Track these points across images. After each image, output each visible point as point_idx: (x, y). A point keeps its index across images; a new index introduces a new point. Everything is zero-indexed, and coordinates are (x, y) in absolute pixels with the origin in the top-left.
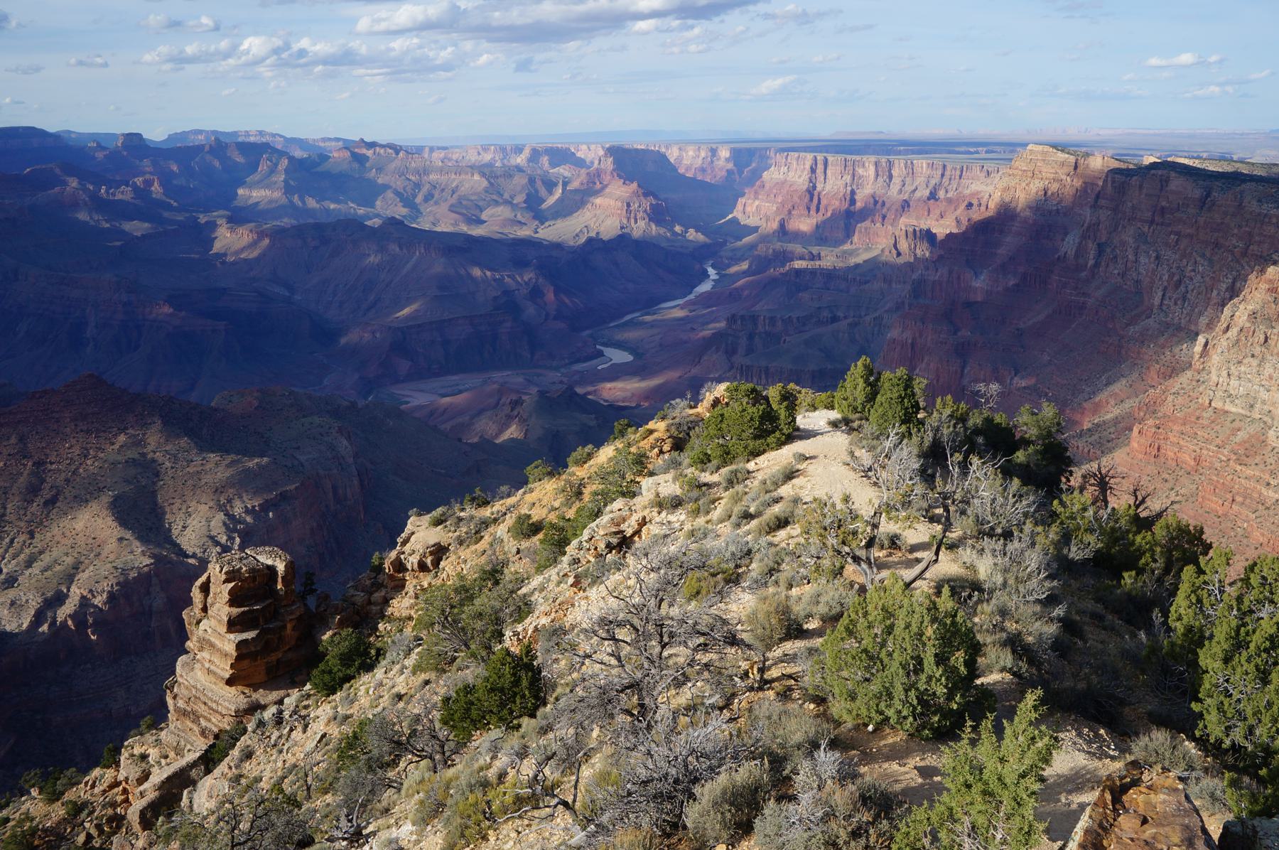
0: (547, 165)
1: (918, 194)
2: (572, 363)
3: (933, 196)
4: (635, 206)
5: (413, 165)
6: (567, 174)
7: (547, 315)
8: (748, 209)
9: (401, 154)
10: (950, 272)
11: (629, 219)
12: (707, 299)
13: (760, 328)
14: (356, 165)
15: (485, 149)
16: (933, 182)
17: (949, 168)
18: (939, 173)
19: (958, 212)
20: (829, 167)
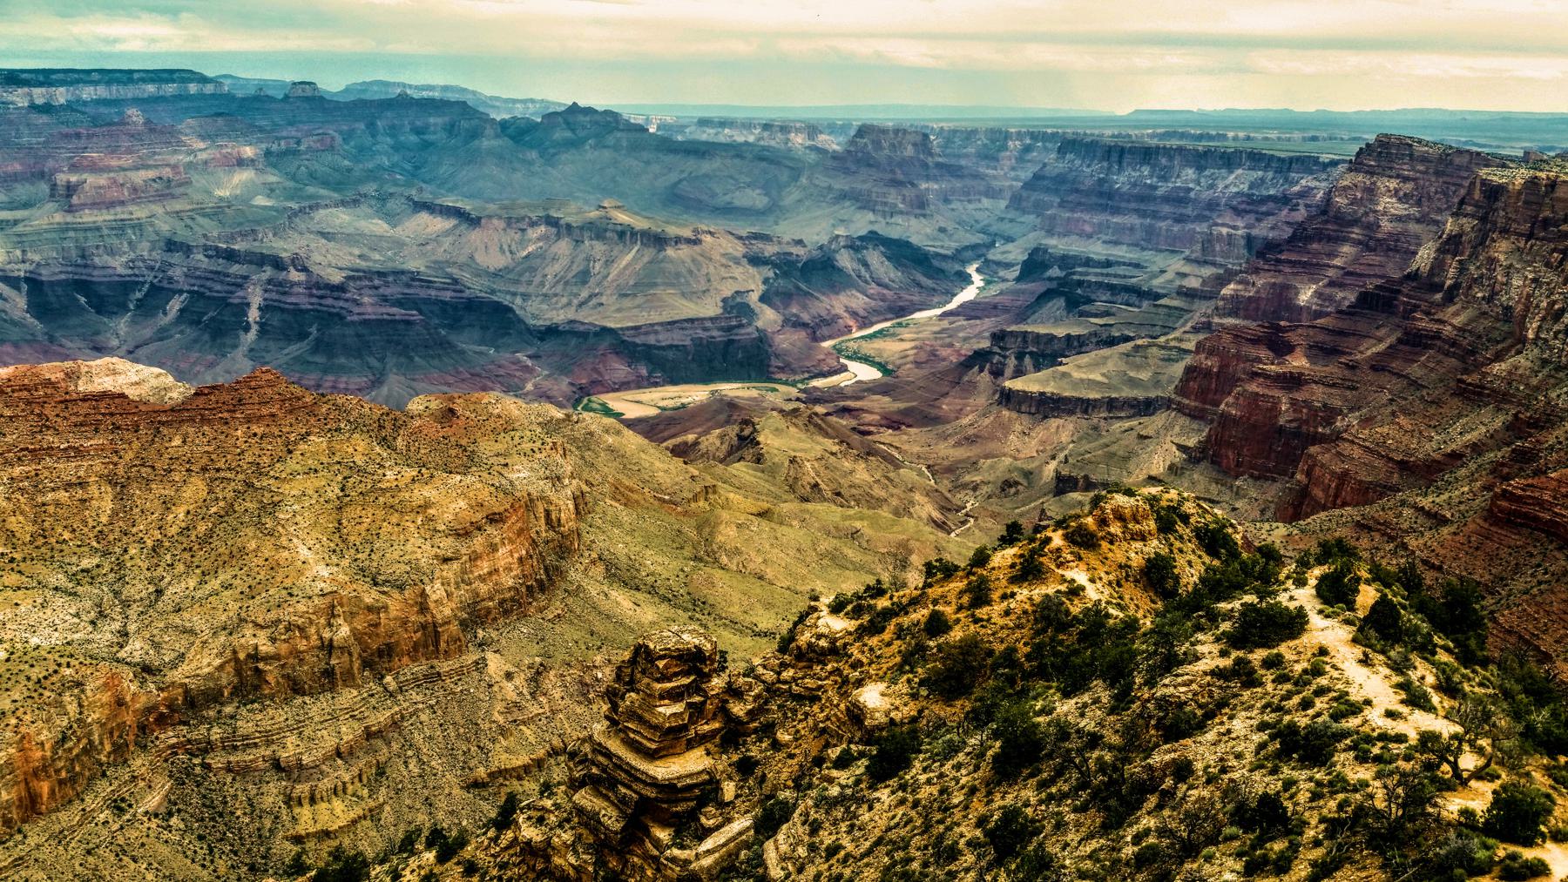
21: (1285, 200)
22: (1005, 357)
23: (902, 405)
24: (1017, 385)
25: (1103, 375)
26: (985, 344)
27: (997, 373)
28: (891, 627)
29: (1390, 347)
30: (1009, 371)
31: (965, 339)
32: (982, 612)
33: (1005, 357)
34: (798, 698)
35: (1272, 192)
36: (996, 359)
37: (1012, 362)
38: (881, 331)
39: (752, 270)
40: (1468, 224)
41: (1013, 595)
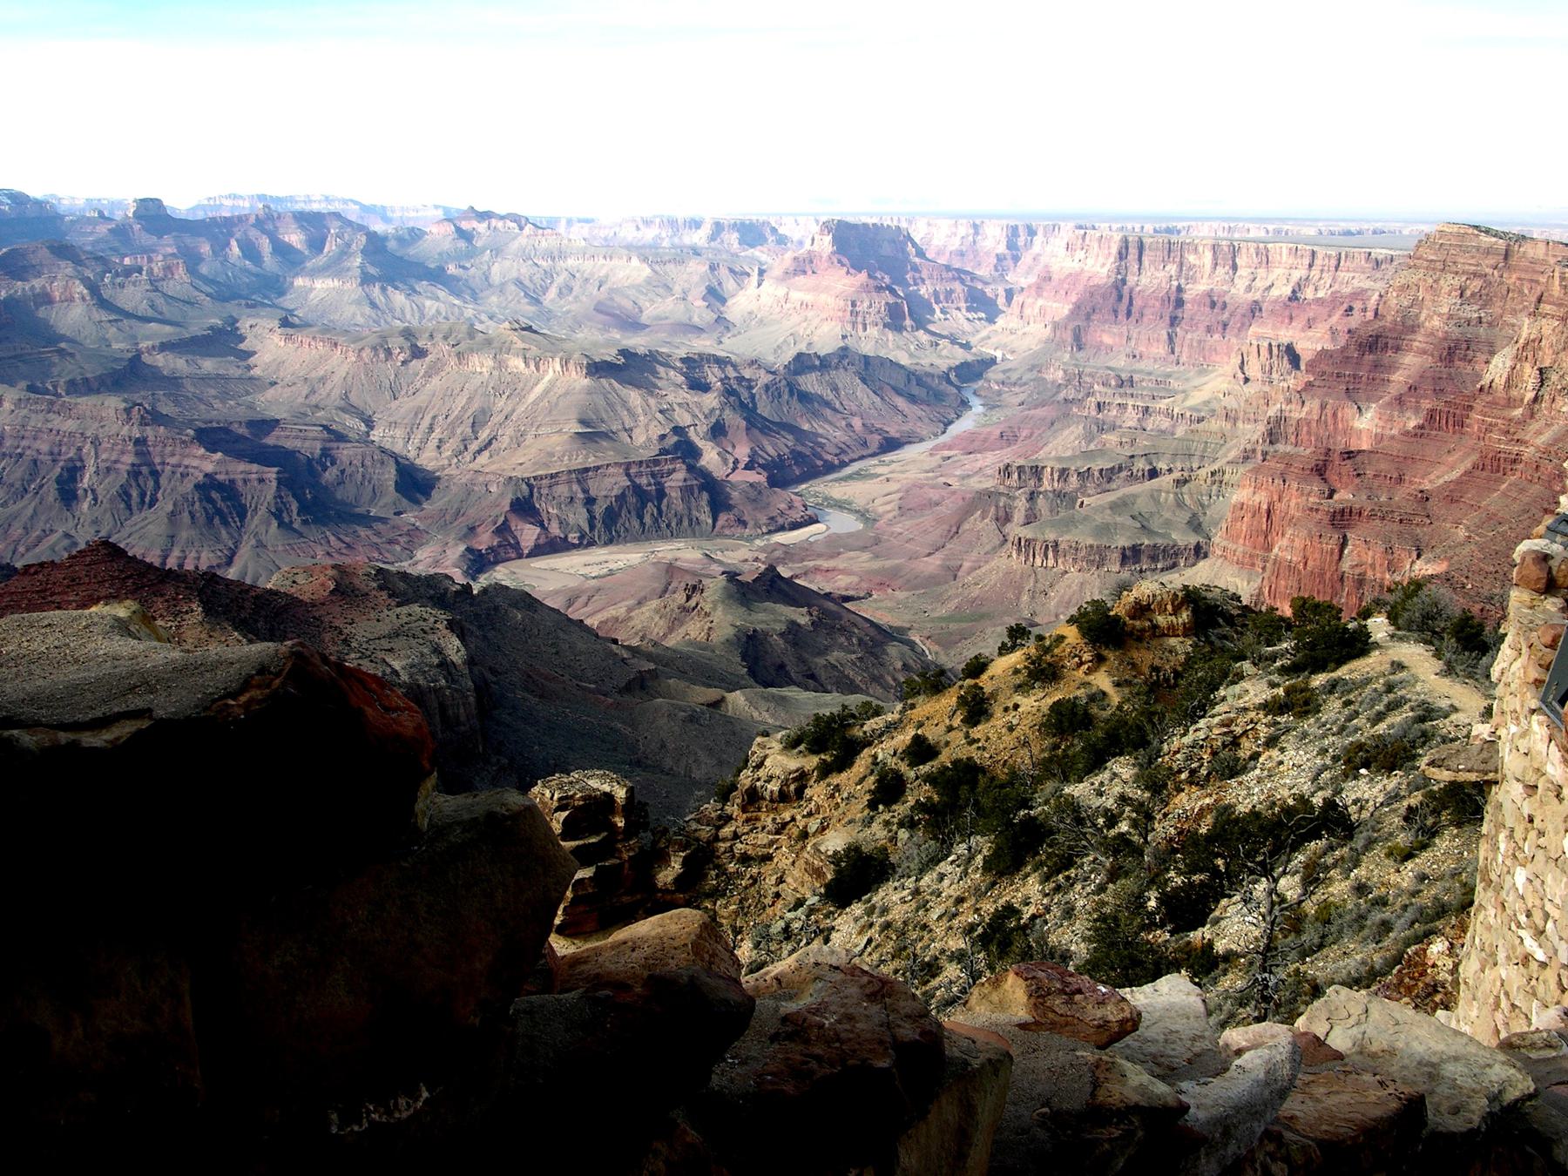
0: (736, 245)
1: (1275, 292)
2: (770, 532)
3: (1294, 297)
4: (862, 307)
5: (544, 244)
6: (764, 258)
7: (736, 462)
8: (1027, 311)
9: (528, 229)
10: (1323, 407)
11: (854, 324)
12: (971, 445)
13: (1046, 485)
14: (462, 244)
15: (648, 223)
16: (1297, 275)
17: (1320, 256)
18: (1307, 261)
19: (1335, 319)
20: (1146, 252)
21: (1334, 301)
22: (1014, 498)
23: (888, 563)
24: (1026, 533)
25: (1133, 517)
26: (989, 484)
27: (1004, 518)
28: (862, 763)
29: (1466, 473)
30: (1019, 516)
31: (963, 478)
32: (978, 732)
33: (1014, 498)
34: (745, 859)
35: (1321, 294)
36: (1003, 500)
37: (1021, 504)
38: (857, 473)
39: (692, 397)
40: (1548, 327)
41: (1016, 707)
